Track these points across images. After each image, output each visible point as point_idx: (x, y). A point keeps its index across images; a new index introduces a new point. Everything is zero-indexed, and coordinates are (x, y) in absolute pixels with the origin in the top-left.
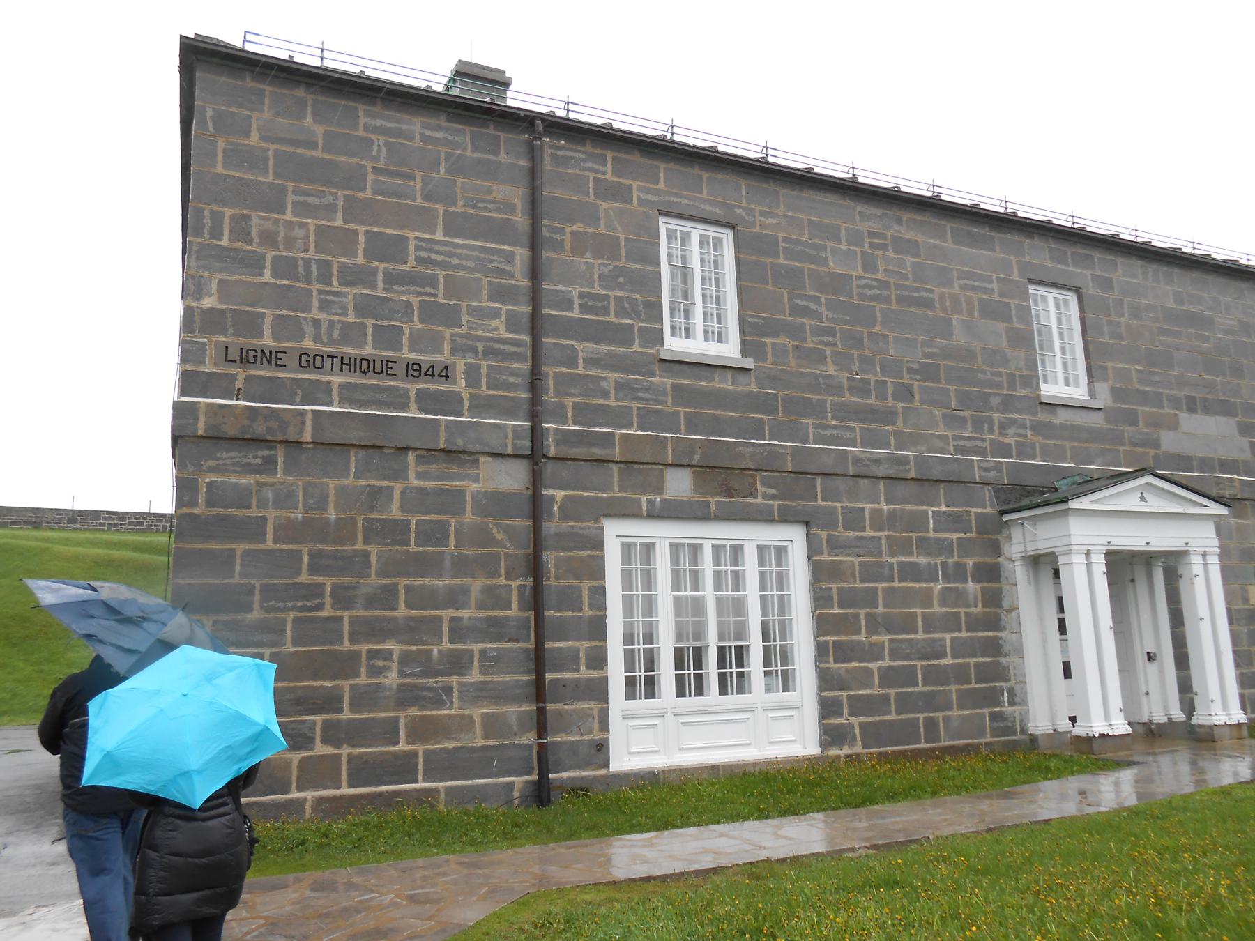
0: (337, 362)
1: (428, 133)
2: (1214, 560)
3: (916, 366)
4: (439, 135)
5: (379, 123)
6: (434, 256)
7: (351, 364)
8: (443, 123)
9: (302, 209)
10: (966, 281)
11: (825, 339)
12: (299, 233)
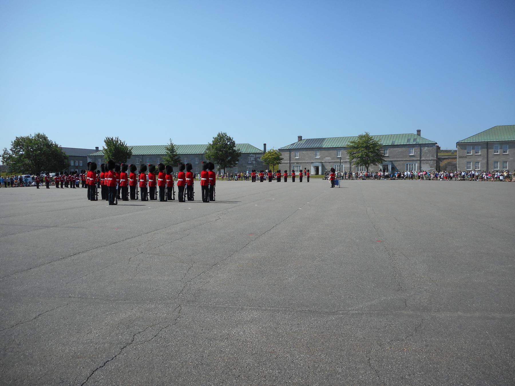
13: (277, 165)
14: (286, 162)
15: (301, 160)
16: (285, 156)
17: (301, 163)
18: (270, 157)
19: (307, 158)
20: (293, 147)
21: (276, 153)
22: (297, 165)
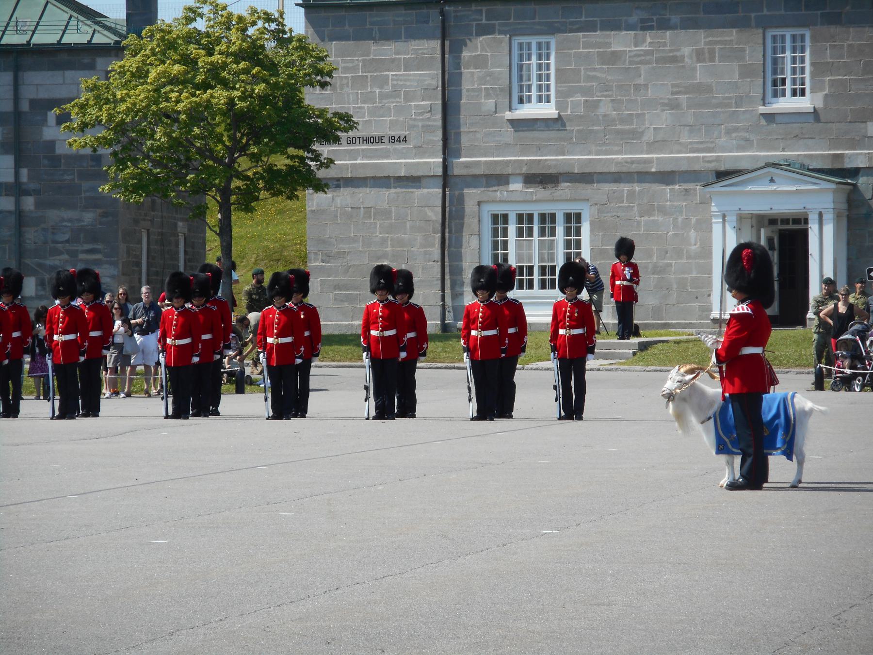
0: (361, 140)
1: (397, 19)
2: (829, 217)
3: (666, 101)
4: (401, 19)
5: (375, 19)
6: (399, 83)
7: (368, 140)
8: (403, 12)
9: (346, 70)
10: (710, 39)
11: (605, 93)
12: (345, 81)
13: (269, 203)
14: (399, 162)
15: (585, 139)
17: (585, 178)
18: (183, 101)
19: (664, 119)
21: (252, 53)
22: (540, 200)
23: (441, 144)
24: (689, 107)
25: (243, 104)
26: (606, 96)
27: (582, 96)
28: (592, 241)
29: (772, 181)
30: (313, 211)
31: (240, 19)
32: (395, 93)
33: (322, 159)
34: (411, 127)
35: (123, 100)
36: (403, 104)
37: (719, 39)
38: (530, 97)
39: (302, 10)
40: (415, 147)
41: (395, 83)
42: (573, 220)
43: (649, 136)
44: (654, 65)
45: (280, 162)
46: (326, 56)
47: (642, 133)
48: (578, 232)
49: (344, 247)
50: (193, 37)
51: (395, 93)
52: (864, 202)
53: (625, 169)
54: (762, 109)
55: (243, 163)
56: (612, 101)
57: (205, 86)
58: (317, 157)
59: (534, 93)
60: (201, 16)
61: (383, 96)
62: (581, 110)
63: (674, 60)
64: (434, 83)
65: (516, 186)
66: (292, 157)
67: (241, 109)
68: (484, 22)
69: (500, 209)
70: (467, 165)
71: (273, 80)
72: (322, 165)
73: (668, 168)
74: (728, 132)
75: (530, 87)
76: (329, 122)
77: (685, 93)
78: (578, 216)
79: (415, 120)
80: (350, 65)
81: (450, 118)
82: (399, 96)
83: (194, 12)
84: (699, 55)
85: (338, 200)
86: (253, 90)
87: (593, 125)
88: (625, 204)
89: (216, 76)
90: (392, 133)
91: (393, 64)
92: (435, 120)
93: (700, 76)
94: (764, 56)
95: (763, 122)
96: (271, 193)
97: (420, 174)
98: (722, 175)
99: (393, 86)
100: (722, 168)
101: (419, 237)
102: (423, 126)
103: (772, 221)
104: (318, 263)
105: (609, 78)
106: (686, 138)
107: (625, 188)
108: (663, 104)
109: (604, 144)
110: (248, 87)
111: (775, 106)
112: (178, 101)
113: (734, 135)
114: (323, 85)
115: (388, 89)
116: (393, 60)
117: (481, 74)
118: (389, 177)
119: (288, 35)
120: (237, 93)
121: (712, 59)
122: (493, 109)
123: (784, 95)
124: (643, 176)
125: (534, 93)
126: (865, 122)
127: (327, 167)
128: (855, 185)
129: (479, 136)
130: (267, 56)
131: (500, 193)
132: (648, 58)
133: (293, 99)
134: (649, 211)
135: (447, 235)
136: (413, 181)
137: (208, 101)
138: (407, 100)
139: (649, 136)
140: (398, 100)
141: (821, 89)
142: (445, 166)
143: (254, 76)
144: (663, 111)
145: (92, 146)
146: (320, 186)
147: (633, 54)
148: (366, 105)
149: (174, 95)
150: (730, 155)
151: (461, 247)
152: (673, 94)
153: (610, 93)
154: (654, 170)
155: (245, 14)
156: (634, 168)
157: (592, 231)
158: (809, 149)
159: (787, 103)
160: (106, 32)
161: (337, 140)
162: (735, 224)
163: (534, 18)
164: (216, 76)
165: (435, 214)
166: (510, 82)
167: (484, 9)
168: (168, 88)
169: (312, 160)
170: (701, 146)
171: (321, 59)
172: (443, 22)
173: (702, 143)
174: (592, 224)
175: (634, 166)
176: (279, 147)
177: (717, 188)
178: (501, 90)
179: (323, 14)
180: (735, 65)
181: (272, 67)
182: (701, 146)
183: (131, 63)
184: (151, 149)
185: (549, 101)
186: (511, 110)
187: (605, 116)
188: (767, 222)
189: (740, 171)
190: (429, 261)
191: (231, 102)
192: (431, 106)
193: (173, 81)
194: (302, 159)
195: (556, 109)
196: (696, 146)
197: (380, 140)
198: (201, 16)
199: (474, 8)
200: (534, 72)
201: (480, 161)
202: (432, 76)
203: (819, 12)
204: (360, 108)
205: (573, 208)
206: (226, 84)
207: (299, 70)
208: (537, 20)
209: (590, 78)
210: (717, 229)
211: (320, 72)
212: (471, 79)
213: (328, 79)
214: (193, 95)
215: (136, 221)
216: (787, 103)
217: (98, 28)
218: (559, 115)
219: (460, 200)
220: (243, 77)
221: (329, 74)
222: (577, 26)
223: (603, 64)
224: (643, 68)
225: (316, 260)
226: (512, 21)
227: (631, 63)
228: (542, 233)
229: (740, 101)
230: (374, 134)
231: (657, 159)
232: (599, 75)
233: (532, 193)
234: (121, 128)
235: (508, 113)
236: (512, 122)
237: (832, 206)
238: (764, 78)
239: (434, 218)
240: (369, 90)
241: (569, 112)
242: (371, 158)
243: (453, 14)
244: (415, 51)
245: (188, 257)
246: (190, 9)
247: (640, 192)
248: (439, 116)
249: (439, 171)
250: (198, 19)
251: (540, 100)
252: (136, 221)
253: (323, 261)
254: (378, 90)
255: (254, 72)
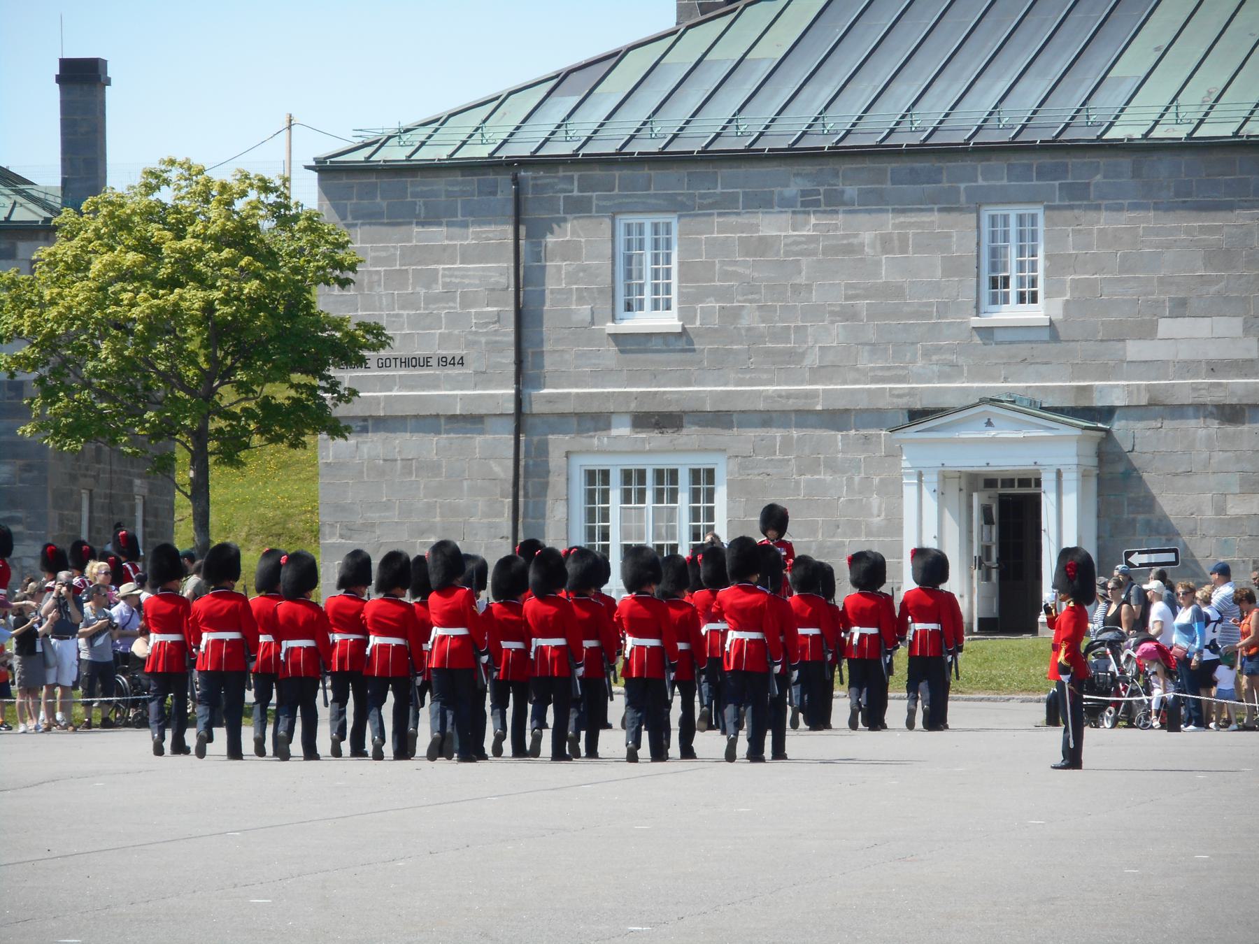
1: (450, 189)
3: (837, 309)
4: (456, 189)
5: (419, 189)
6: (454, 280)
7: (408, 362)
8: (460, 178)
9: (377, 261)
11: (750, 297)
12: (375, 278)
13: (264, 455)
14: (454, 394)
16: (425, 299)
17: (720, 419)
18: (140, 304)
19: (835, 335)
20: (592, 125)
21: (240, 237)
22: (655, 452)
23: (512, 368)
24: (871, 317)
25: (227, 310)
26: (751, 301)
27: (717, 301)
28: (729, 510)
29: (989, 424)
30: (328, 464)
31: (224, 187)
32: (448, 295)
33: (341, 389)
34: (470, 344)
35: (53, 302)
36: (459, 311)
37: (913, 220)
38: (641, 302)
39: (316, 175)
40: (476, 373)
41: (448, 280)
42: (703, 479)
43: (813, 359)
44: (821, 257)
45: (281, 393)
46: (348, 242)
47: (803, 355)
48: (710, 497)
49: (374, 516)
50: (154, 214)
51: (448, 295)
52: (1121, 456)
53: (777, 407)
54: (975, 321)
55: (227, 395)
56: (760, 308)
57: (172, 283)
58: (333, 387)
59: (648, 296)
60: (167, 182)
61: (430, 300)
62: (715, 322)
63: (849, 249)
64: (503, 280)
65: (622, 430)
66: (296, 387)
67: (224, 316)
68: (576, 193)
69: (597, 463)
70: (551, 399)
71: (270, 275)
72: (340, 398)
73: (840, 405)
74: (927, 354)
75: (641, 287)
76: (347, 334)
77: (866, 298)
78: (710, 473)
79: (476, 333)
80: (384, 254)
81: (527, 332)
82: (454, 300)
83: (157, 177)
84: (886, 243)
85: (365, 449)
86: (241, 289)
87: (732, 343)
88: (778, 457)
89: (186, 271)
90: (444, 353)
91: (444, 254)
92: (505, 334)
93: (885, 275)
94: (978, 244)
95: (977, 340)
96: (267, 439)
97: (483, 411)
98: (917, 416)
99: (445, 285)
100: (919, 406)
101: (481, 503)
102: (487, 343)
103: (990, 483)
104: (335, 540)
105: (756, 275)
106: (865, 362)
107: (778, 434)
108: (832, 313)
109: (748, 370)
110: (234, 285)
111: (995, 316)
112: (132, 305)
113: (934, 358)
114: (344, 283)
115: (438, 289)
116: (445, 248)
117: (570, 269)
118: (437, 416)
119: (294, 211)
120: (217, 294)
121: (903, 250)
122: (589, 318)
123: (1006, 301)
124: (804, 417)
125: (648, 296)
126: (1124, 340)
127: (348, 402)
128: (1108, 431)
129: (567, 356)
130: (261, 241)
131: (598, 440)
132: (812, 246)
133: (298, 303)
134: (813, 466)
135: (521, 500)
136: (471, 421)
137: (176, 305)
138: (464, 305)
139: (813, 359)
140: (451, 304)
141: (1060, 293)
142: (519, 400)
143: (242, 269)
144: (833, 322)
145: (8, 369)
146: (337, 429)
147: (789, 241)
148: (405, 313)
149: (126, 296)
150: (927, 387)
151: (543, 516)
152: (846, 299)
153: (756, 296)
154: (819, 408)
155: (230, 180)
156: (791, 404)
157: (730, 495)
158: (1043, 379)
159: (1011, 313)
160: (31, 206)
161: (361, 362)
162: (935, 486)
163: (648, 188)
164: (186, 271)
165: (504, 470)
166: (613, 281)
167: (576, 175)
168: (118, 286)
169: (326, 391)
170: (887, 374)
171: (343, 246)
172: (517, 194)
173: (889, 368)
174: (731, 484)
175: (791, 401)
176: (280, 373)
177: (911, 433)
178: (601, 291)
179: (344, 180)
180: (937, 258)
181: (270, 258)
182: (887, 374)
183: (64, 249)
184: (93, 373)
185: (668, 308)
186: (614, 320)
187: (749, 329)
188: (981, 484)
189: (943, 410)
190: (495, 537)
191: (209, 308)
192: (499, 313)
193: (126, 276)
194: (312, 390)
195: (680, 320)
196: (880, 373)
197: (426, 362)
198: (167, 182)
199: (561, 174)
200: (648, 266)
201: (569, 394)
202: (500, 271)
203: (1057, 183)
204: (397, 316)
205: (702, 462)
206: (203, 282)
207: (309, 262)
208: (652, 192)
209: (726, 276)
210: (910, 493)
211: (339, 265)
212: (558, 276)
213: (350, 275)
214: (155, 296)
215: (73, 478)
216: (1011, 313)
217: (20, 199)
218: (684, 329)
219: (543, 450)
220: (226, 271)
221: (352, 268)
222: (710, 201)
223: (747, 255)
224: (804, 261)
225: (332, 535)
226: (616, 191)
227: (787, 254)
228: (659, 497)
229: (943, 309)
230: (419, 353)
231: (824, 391)
232: (740, 270)
233: (643, 440)
234: (50, 343)
235: (610, 324)
236: (616, 338)
237: (1075, 460)
238: (978, 276)
239: (502, 475)
240: (410, 290)
241: (698, 324)
242: (412, 388)
243: (531, 183)
244: (477, 236)
245: (148, 530)
246: (152, 173)
247: (799, 438)
248: (511, 329)
249: (510, 408)
250: (164, 188)
251: (656, 306)
252: (73, 478)
253: (342, 536)
254: (423, 291)
255: (242, 263)
